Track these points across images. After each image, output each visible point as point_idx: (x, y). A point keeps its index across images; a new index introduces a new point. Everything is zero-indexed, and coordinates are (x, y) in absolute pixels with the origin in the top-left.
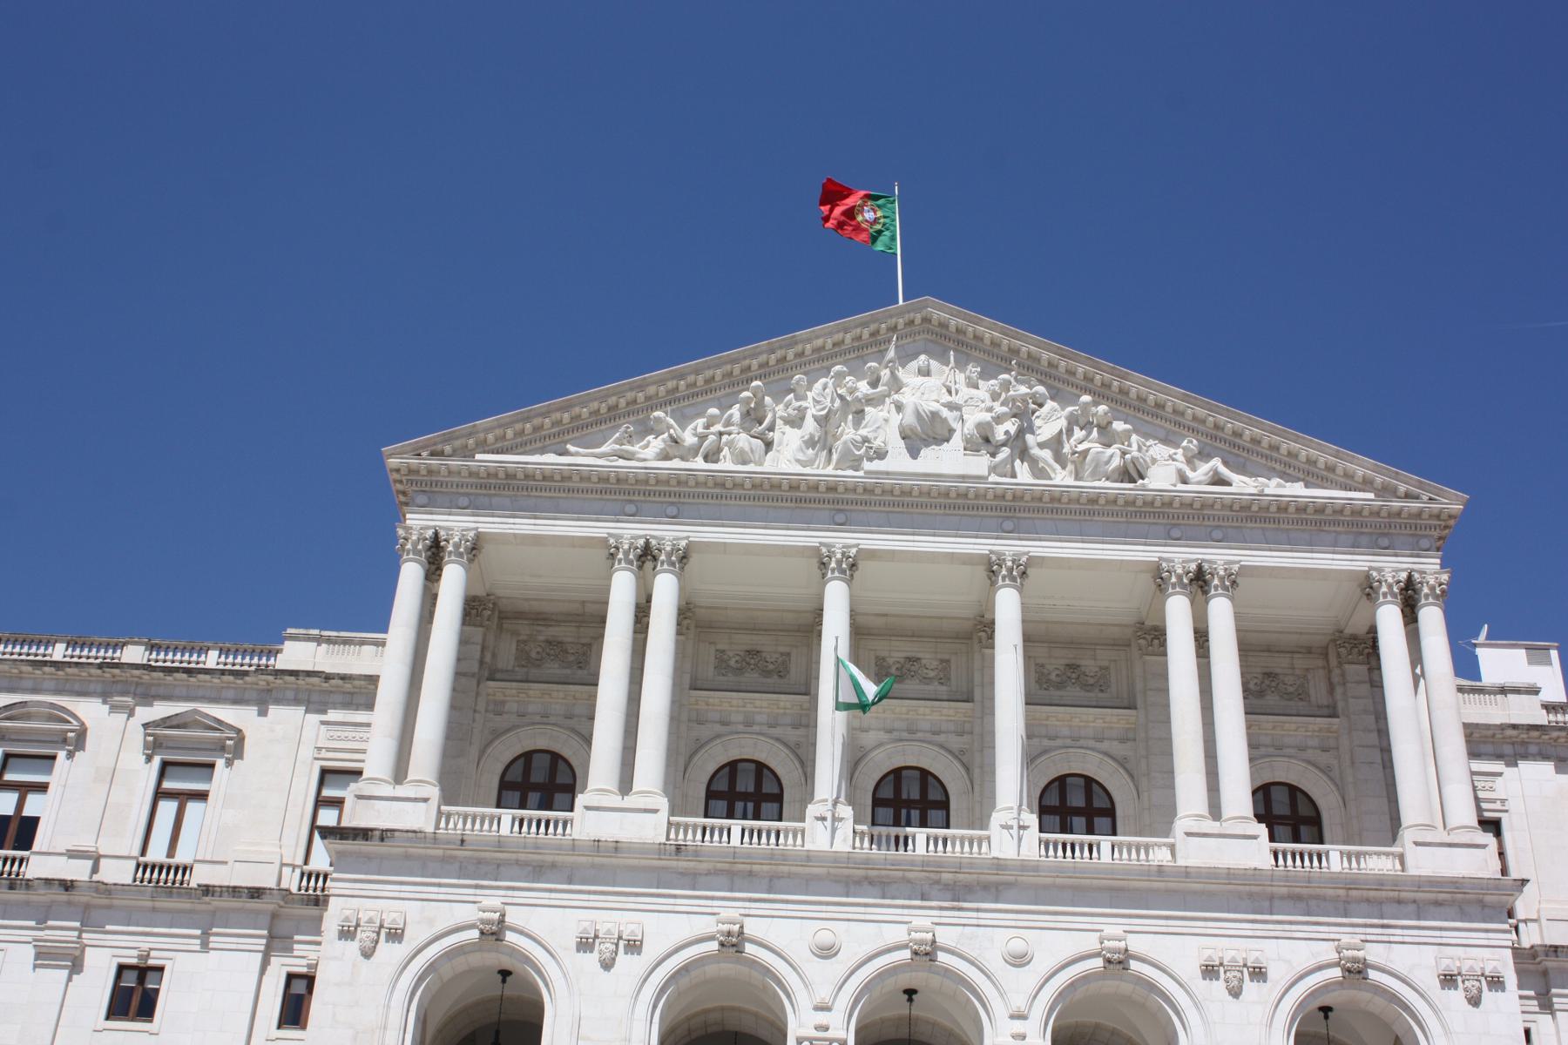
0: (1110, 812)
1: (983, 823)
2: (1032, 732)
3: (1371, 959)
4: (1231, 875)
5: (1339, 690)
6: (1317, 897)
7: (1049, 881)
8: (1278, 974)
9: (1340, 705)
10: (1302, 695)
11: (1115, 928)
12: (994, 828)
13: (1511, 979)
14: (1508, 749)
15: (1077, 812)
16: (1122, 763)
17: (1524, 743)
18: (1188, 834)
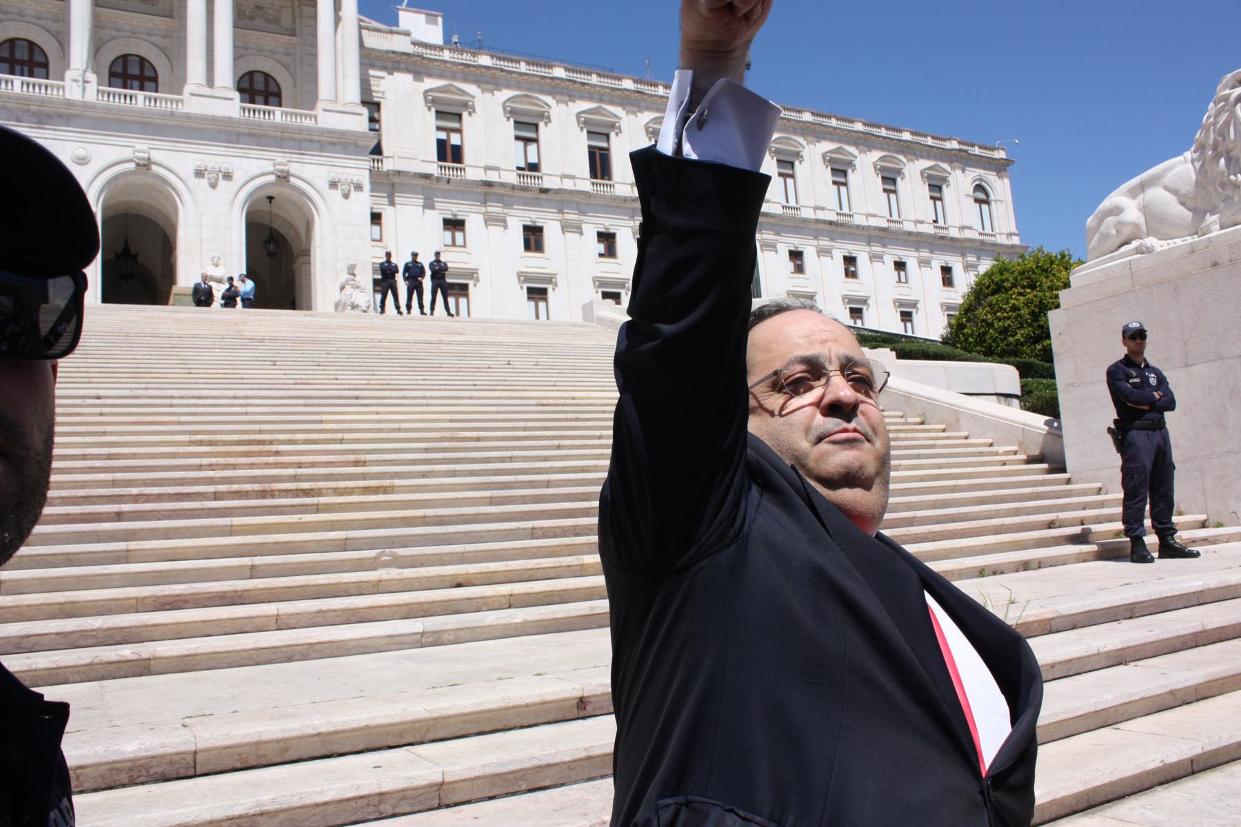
0: (155, 79)
1: (63, 79)
2: (97, 25)
3: (292, 171)
4: (214, 119)
5: (298, 21)
6: (264, 136)
7: (103, 115)
8: (239, 177)
9: (298, 29)
10: (277, 21)
11: (141, 147)
12: (67, 83)
13: (367, 186)
14: (390, 65)
15: (134, 77)
16: (163, 50)
17: (398, 62)
18: (193, 95)
